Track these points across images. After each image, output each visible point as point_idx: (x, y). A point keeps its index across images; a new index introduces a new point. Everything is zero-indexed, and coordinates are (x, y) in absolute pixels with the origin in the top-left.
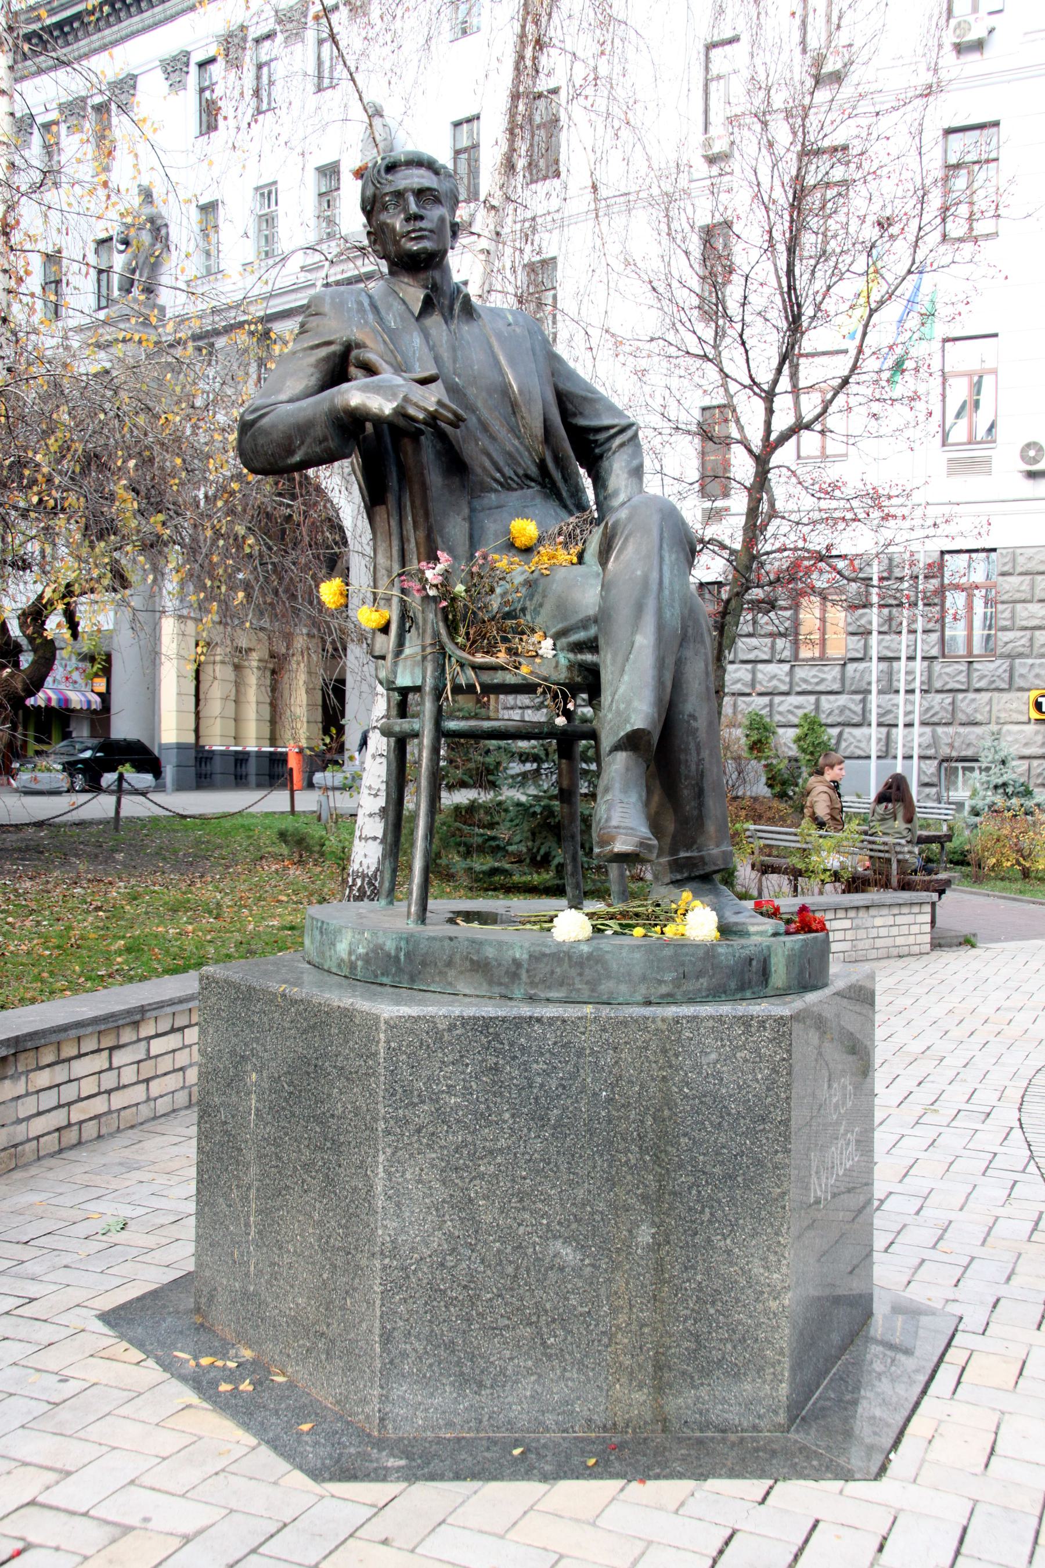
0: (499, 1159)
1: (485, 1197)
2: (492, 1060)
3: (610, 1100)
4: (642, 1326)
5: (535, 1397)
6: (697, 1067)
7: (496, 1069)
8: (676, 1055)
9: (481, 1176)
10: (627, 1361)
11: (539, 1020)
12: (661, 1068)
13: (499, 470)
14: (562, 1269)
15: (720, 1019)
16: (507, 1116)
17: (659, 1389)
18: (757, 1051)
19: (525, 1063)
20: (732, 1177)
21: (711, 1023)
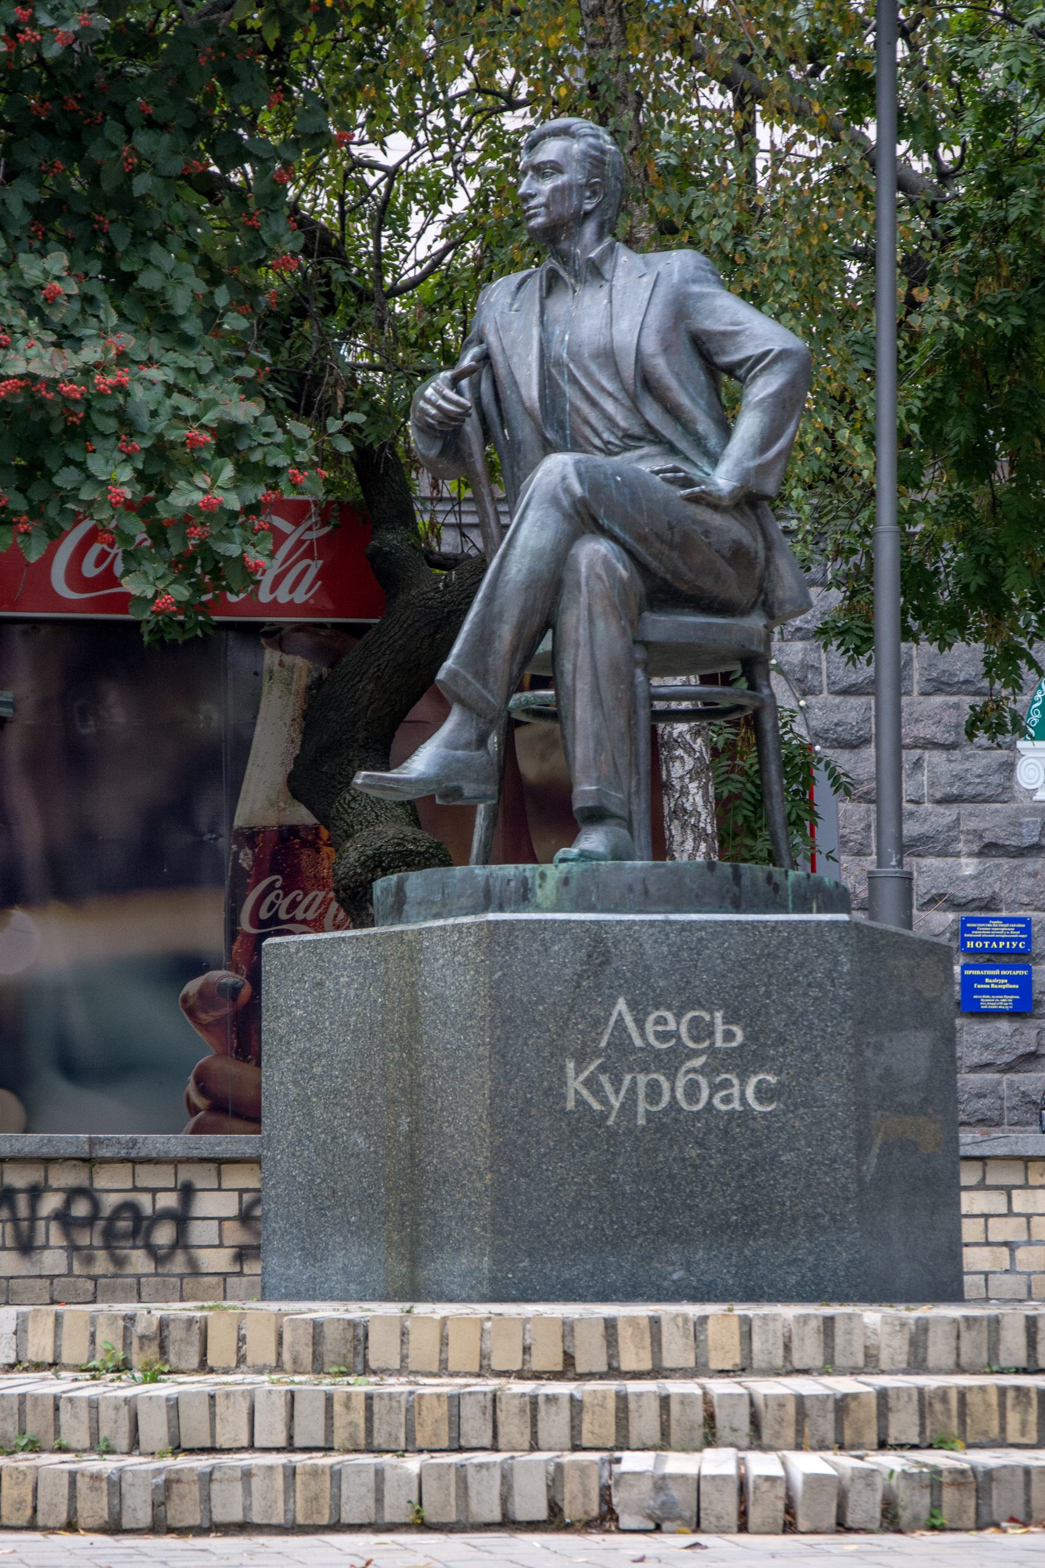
0: (324, 1062)
1: (317, 1095)
2: (319, 976)
3: (383, 1005)
4: (404, 1205)
5: (345, 1268)
6: (432, 972)
7: (320, 984)
8: (420, 963)
9: (313, 1078)
10: (396, 1237)
11: (343, 939)
12: (411, 975)
13: (598, 435)
14: (358, 1155)
15: (443, 928)
16: (327, 1024)
17: (414, 1262)
18: (466, 955)
19: (337, 977)
20: (453, 1069)
21: (439, 933)
